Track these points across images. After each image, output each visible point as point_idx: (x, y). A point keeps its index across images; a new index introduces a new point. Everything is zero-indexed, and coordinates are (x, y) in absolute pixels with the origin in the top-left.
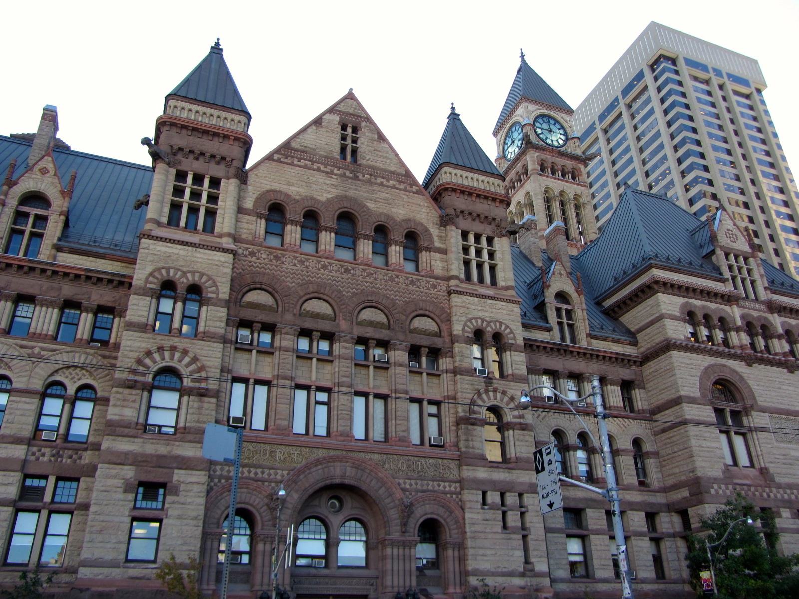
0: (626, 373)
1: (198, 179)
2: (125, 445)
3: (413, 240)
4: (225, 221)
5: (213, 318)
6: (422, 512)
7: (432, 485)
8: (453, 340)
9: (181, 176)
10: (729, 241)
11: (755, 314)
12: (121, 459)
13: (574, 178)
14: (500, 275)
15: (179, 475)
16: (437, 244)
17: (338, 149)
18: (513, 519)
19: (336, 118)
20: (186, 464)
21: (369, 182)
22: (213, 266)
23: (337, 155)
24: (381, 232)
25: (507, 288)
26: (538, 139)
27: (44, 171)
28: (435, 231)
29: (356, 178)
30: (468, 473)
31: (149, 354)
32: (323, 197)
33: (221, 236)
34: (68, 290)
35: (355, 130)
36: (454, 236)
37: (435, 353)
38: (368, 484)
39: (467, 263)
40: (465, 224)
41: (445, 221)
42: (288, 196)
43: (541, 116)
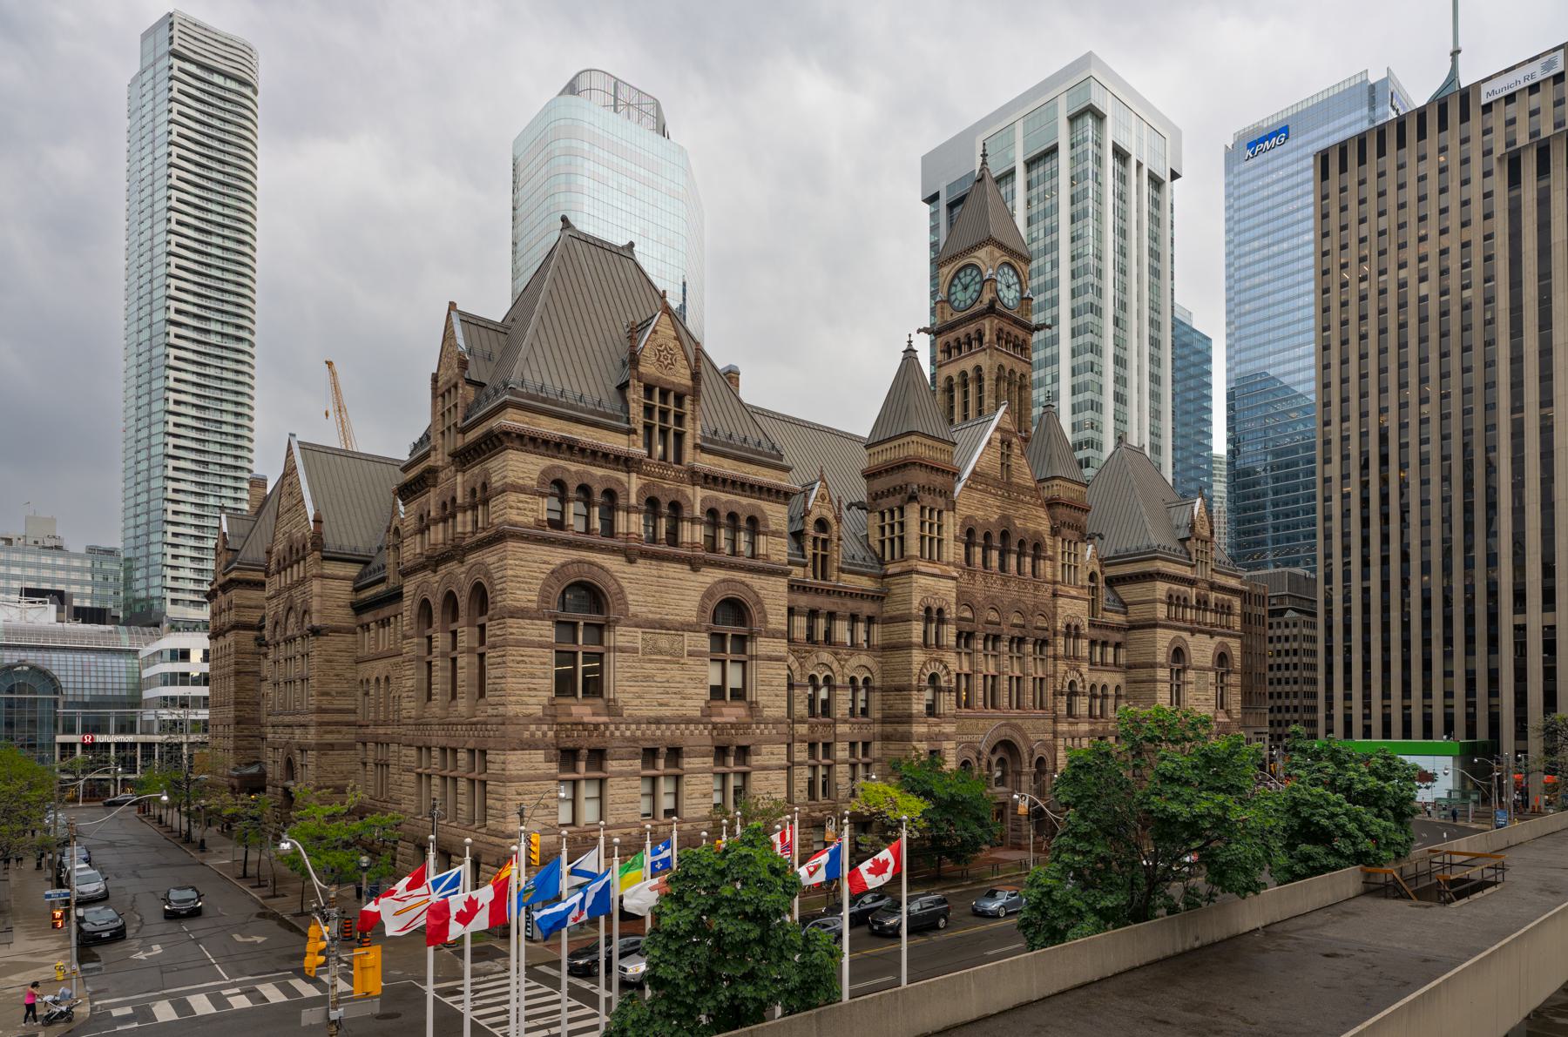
5: (949, 634)
16: (1050, 553)
28: (1048, 541)
29: (1009, 497)
41: (1055, 532)
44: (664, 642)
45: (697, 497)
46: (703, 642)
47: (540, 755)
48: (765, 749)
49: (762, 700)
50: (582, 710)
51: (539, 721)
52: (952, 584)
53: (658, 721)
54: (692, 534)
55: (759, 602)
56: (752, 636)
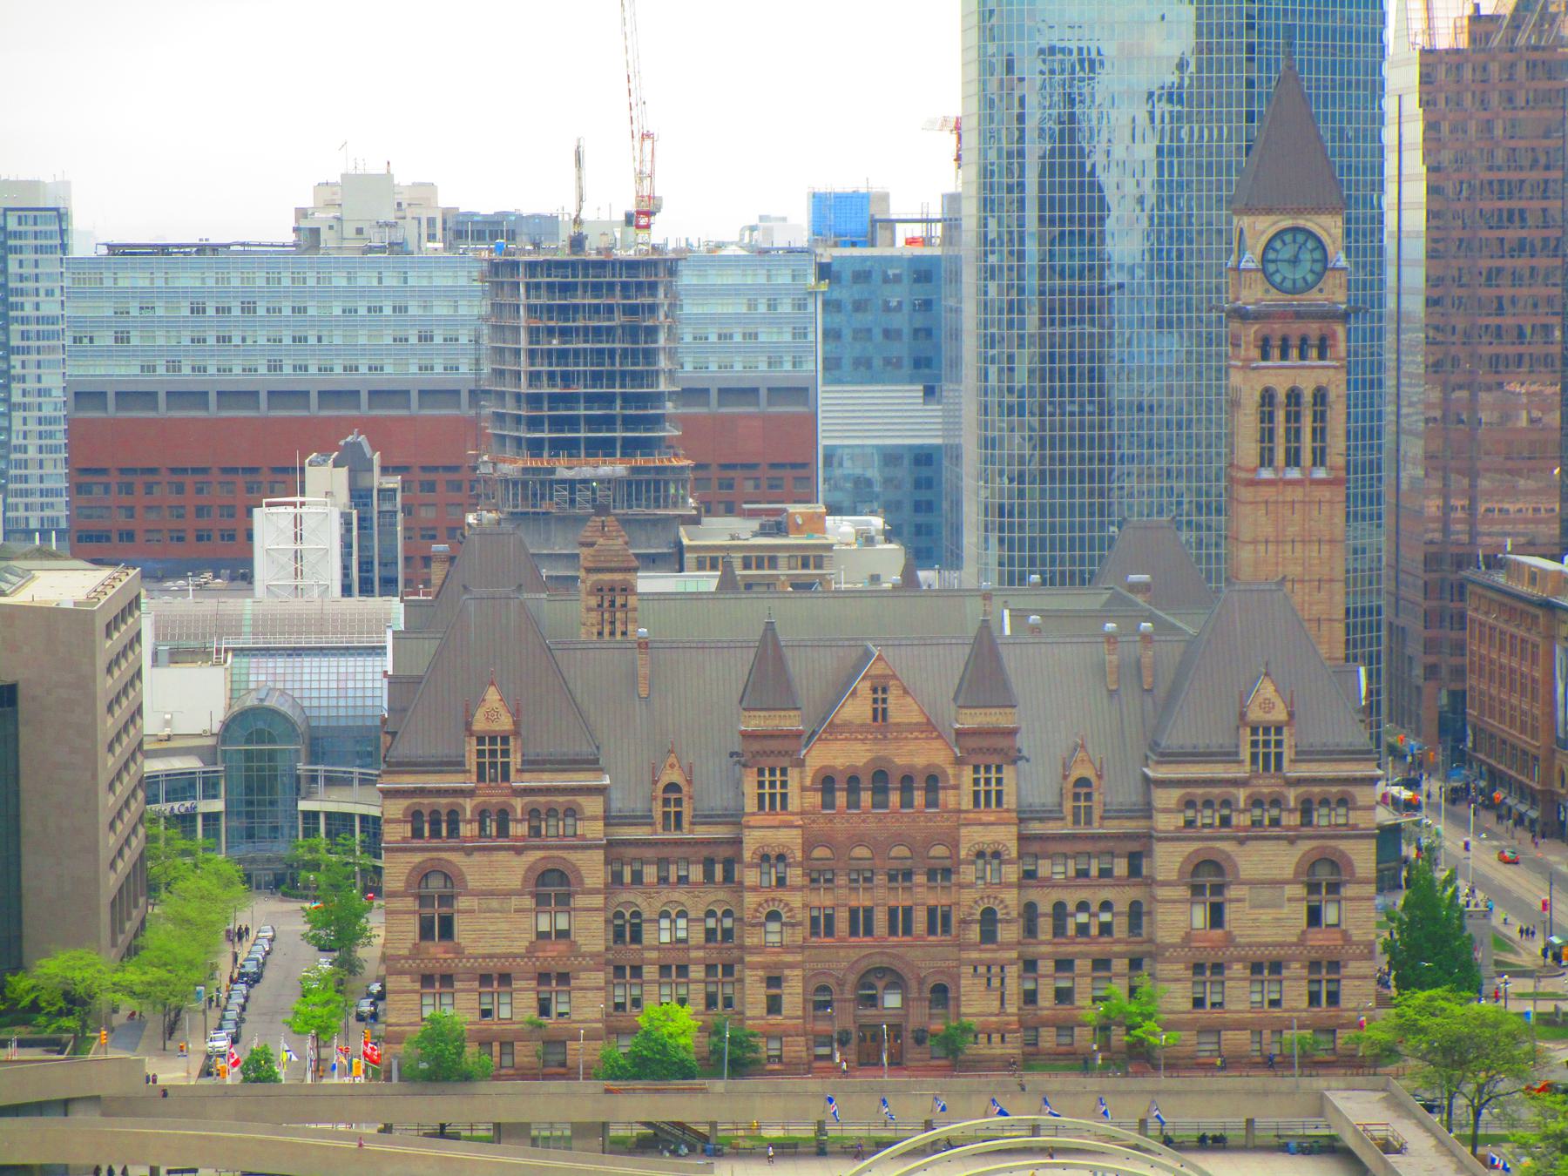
0: (1135, 846)
1: (772, 772)
2: (756, 959)
3: (933, 782)
4: (794, 803)
5: (795, 875)
6: (931, 982)
7: (939, 964)
8: (959, 863)
9: (761, 772)
10: (1261, 713)
11: (1266, 790)
12: (753, 967)
13: (1322, 356)
14: (1005, 799)
15: (787, 972)
16: (952, 782)
17: (870, 713)
18: (996, 982)
19: (868, 684)
20: (791, 966)
21: (896, 738)
22: (790, 839)
23: (869, 721)
24: (907, 783)
25: (1008, 811)
26: (1268, 285)
27: (672, 766)
28: (950, 771)
29: (885, 738)
30: (964, 955)
31: (760, 905)
32: (861, 762)
33: (793, 814)
34: (705, 852)
35: (884, 690)
36: (968, 774)
37: (947, 872)
38: (896, 965)
39: (976, 794)
40: (978, 759)
42: (833, 768)
43: (1279, 234)
44: (494, 904)
45: (518, 804)
46: (529, 902)
47: (406, 979)
48: (583, 975)
49: (580, 941)
50: (436, 948)
51: (406, 958)
52: (799, 831)
53: (491, 956)
54: (518, 829)
55: (577, 871)
56: (569, 895)
